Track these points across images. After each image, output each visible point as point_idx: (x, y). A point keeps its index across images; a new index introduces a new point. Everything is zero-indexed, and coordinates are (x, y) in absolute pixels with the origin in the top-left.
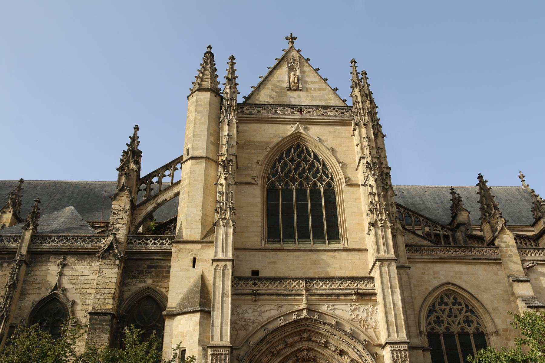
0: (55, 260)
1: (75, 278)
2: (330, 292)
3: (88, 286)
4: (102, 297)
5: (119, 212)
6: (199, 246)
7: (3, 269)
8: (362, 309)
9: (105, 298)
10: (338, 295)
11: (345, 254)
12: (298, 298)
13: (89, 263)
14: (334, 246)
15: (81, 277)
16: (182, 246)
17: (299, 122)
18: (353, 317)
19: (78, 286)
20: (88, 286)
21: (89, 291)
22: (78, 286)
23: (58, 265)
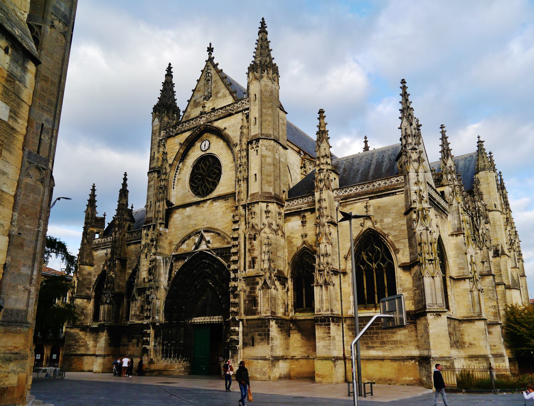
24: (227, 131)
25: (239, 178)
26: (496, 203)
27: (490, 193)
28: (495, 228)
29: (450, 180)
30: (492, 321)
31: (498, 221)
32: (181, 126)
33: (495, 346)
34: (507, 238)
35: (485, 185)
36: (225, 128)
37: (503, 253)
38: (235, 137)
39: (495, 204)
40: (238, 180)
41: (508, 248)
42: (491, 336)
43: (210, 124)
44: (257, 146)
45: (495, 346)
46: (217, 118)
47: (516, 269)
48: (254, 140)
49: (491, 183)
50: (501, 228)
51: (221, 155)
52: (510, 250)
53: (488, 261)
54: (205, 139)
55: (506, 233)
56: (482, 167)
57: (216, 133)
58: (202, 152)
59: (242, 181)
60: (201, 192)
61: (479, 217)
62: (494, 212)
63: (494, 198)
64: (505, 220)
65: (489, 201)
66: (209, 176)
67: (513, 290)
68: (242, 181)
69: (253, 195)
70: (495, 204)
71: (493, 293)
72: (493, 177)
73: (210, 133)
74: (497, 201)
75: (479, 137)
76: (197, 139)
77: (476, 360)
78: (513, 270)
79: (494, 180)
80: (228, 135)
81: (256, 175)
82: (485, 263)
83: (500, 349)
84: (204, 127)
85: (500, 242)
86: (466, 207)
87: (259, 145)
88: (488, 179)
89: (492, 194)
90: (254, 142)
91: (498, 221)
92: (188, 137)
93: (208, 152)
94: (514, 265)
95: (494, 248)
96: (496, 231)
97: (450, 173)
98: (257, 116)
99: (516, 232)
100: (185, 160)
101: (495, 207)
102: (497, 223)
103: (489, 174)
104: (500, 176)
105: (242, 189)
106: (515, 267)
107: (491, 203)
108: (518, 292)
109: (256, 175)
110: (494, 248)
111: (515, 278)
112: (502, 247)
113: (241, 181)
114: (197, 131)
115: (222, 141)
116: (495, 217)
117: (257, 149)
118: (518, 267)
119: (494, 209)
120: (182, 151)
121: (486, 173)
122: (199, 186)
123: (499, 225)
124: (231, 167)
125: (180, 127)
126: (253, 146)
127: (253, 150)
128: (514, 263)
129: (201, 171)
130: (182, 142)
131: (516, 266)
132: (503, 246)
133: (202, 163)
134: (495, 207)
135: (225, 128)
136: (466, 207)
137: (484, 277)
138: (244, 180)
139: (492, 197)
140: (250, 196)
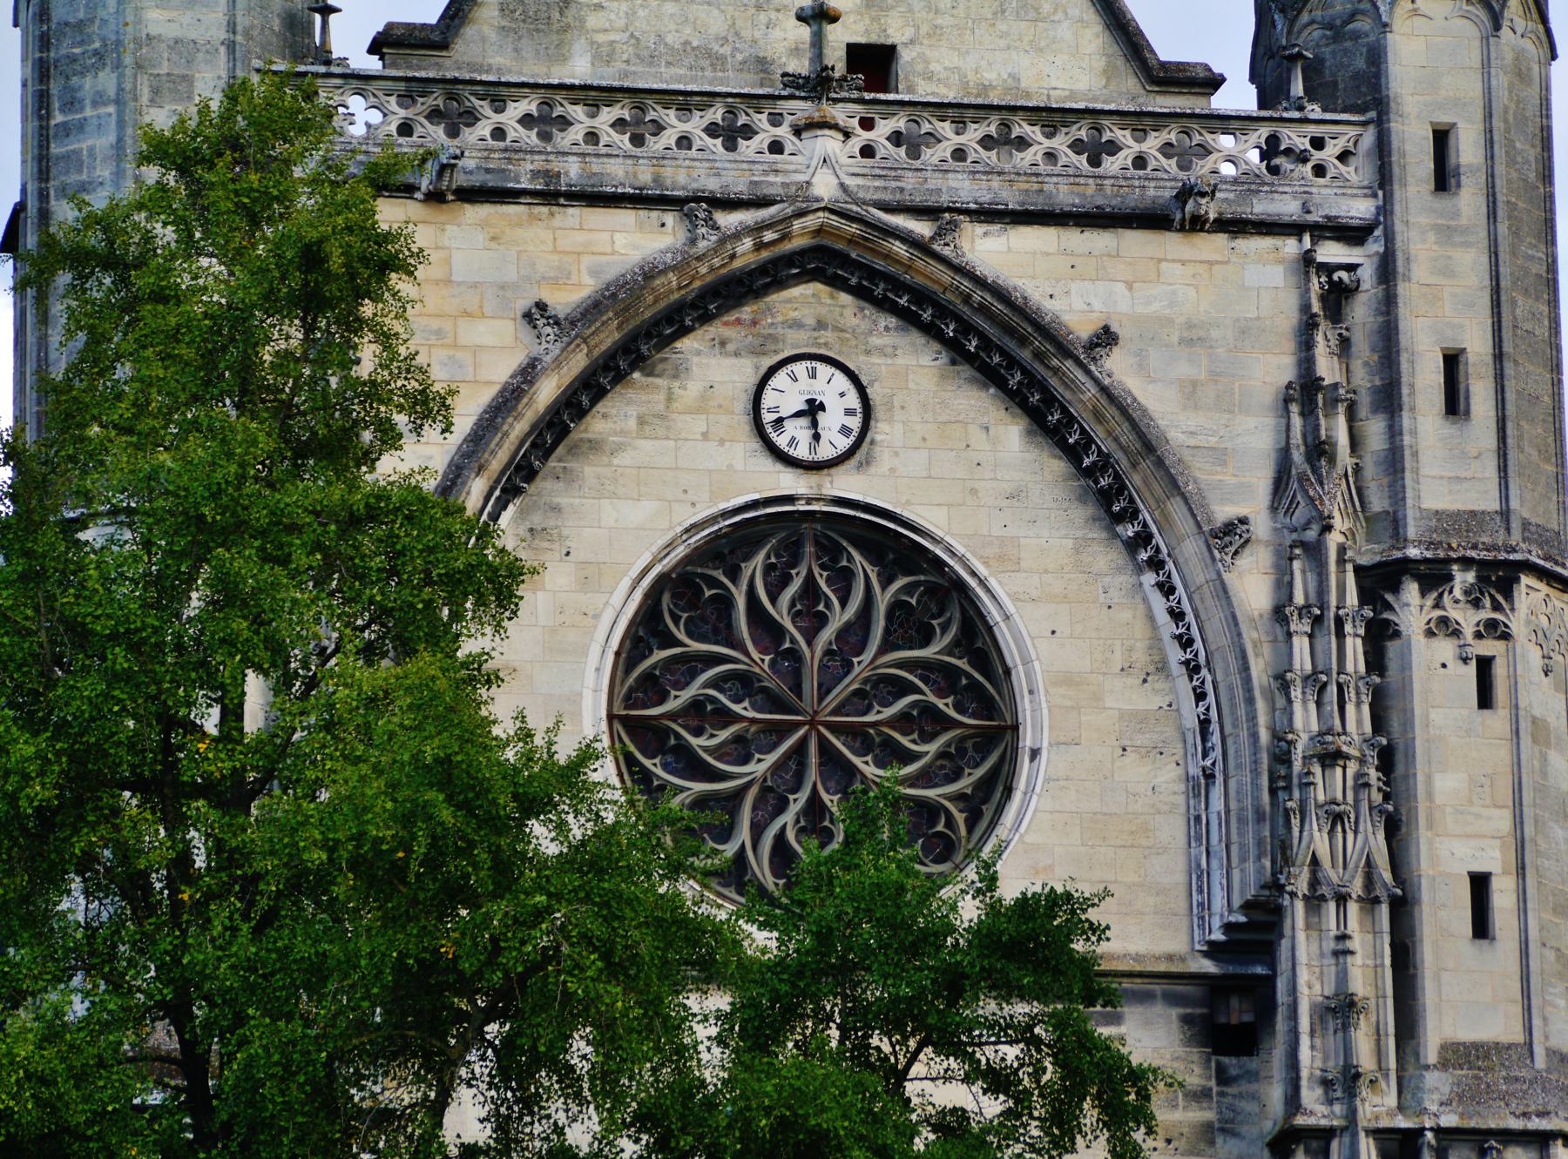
24: (1118, 367)
25: (1331, 874)
32: (527, 120)
36: (1106, 338)
38: (1220, 456)
40: (1314, 883)
43: (922, 228)
44: (1492, 625)
46: (1011, 198)
48: (1466, 562)
51: (1008, 560)
54: (796, 341)
57: (966, 328)
58: (767, 464)
59: (1353, 908)
60: (762, 868)
66: (861, 738)
68: (1353, 908)
69: (1459, 1055)
73: (860, 293)
76: (706, 318)
80: (1145, 411)
81: (1480, 884)
84: (819, 231)
87: (1517, 624)
90: (1463, 579)
92: (649, 273)
93: (847, 484)
98: (1477, 346)
100: (544, 488)
105: (1359, 985)
109: (1480, 884)
113: (1342, 899)
114: (748, 243)
115: (1011, 433)
117: (1488, 647)
120: (547, 391)
122: (740, 793)
124: (1140, 719)
125: (515, 132)
126: (1454, 613)
127: (1445, 649)
129: (759, 661)
130: (563, 300)
133: (756, 565)
135: (1106, 338)
138: (1370, 901)
140: (1444, 1064)
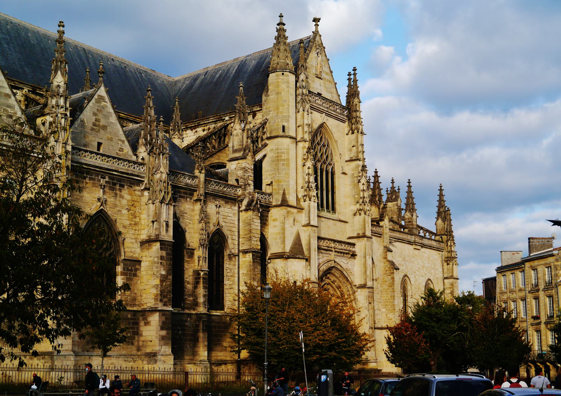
0: (214, 201)
1: (225, 217)
2: (341, 251)
3: (232, 225)
4: (255, 240)
5: (249, 170)
6: (295, 211)
7: (188, 203)
8: (350, 263)
9: (257, 241)
10: (344, 253)
11: (339, 223)
12: (331, 252)
13: (231, 207)
14: (335, 216)
15: (228, 218)
16: (289, 209)
17: (325, 113)
18: (347, 267)
19: (227, 224)
20: (232, 225)
21: (233, 229)
22: (227, 224)
23: (216, 206)
26: (285, 124)
27: (278, 108)
28: (277, 165)
29: (53, 107)
30: (152, 306)
31: (283, 153)
33: (151, 341)
34: (304, 178)
35: (273, 96)
37: (284, 203)
39: (284, 127)
41: (303, 195)
42: (148, 328)
45: (151, 341)
47: (310, 228)
49: (283, 93)
50: (288, 165)
52: (305, 198)
53: (158, 220)
55: (303, 172)
56: (275, 66)
61: (159, 154)
62: (279, 139)
63: (283, 116)
64: (305, 150)
65: (275, 121)
67: (289, 260)
70: (284, 127)
71: (157, 267)
72: (288, 82)
74: (288, 121)
75: (281, 16)
77: (43, 358)
78: (305, 228)
79: (288, 87)
82: (155, 223)
83: (155, 346)
85: (282, 186)
86: (146, 139)
88: (278, 86)
89: (281, 109)
91: (283, 153)
94: (307, 222)
95: (251, 196)
96: (278, 170)
97: (55, 96)
99: (364, 167)
101: (284, 131)
102: (281, 156)
103: (282, 77)
104: (355, 74)
106: (308, 225)
107: (278, 125)
108: (303, 262)
110: (251, 196)
111: (304, 242)
112: (284, 194)
116: (280, 147)
118: (312, 223)
119: (281, 133)
121: (277, 76)
123: (284, 160)
128: (307, 219)
131: (309, 223)
132: (286, 192)
134: (284, 131)
136: (146, 139)
137: (152, 243)
139: (280, 114)
